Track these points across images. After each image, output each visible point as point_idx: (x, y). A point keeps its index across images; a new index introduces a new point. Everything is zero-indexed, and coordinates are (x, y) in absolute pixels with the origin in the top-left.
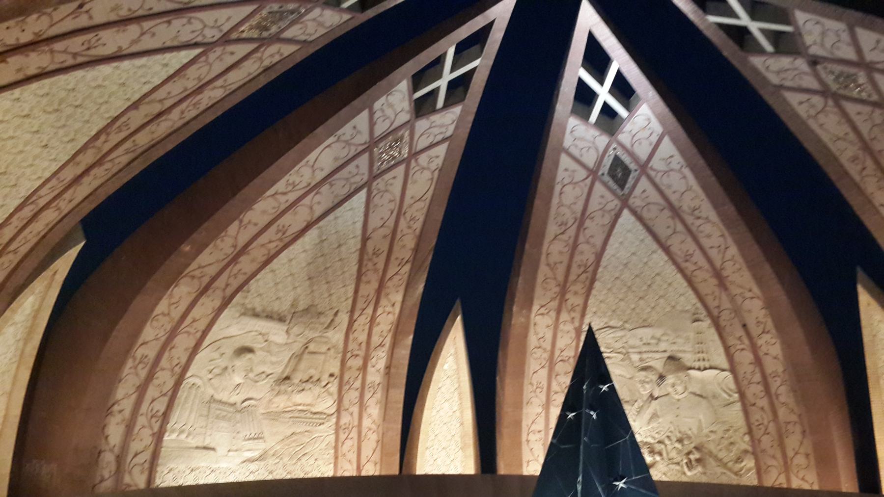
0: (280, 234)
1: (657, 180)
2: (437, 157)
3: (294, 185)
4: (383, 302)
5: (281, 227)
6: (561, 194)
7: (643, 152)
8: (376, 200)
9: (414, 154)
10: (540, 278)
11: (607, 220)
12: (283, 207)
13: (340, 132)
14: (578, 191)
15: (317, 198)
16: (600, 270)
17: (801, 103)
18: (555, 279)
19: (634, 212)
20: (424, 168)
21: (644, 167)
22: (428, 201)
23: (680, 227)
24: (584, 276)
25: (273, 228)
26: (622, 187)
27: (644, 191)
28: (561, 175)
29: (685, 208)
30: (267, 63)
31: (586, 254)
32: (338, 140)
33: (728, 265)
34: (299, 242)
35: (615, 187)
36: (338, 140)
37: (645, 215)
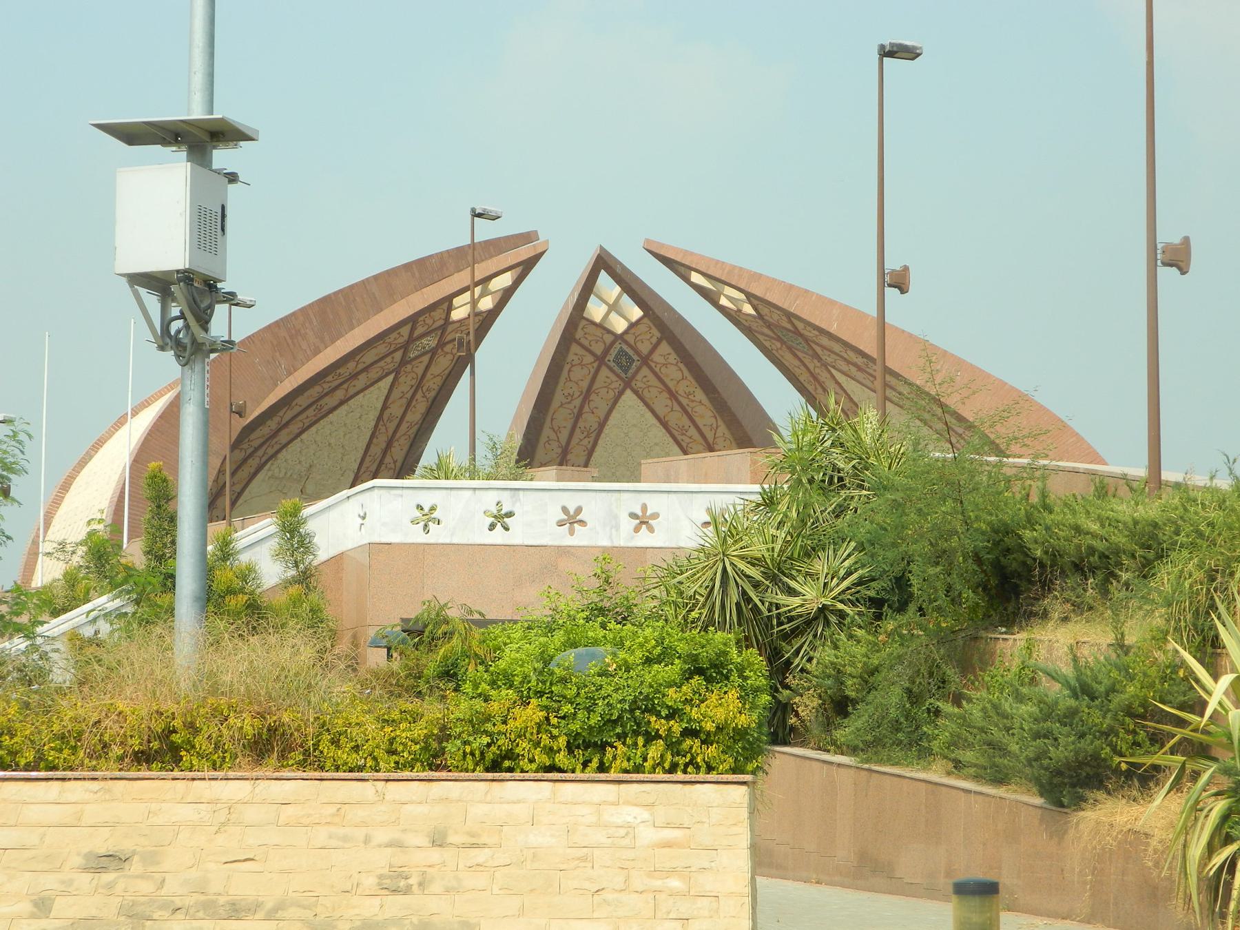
1: (657, 370)
4: (388, 460)
7: (644, 348)
8: (402, 379)
9: (441, 344)
10: (543, 439)
11: (611, 394)
14: (585, 371)
15: (355, 382)
19: (636, 392)
21: (646, 360)
24: (586, 440)
26: (626, 372)
28: (571, 357)
31: (589, 421)
35: (619, 371)
37: (646, 394)
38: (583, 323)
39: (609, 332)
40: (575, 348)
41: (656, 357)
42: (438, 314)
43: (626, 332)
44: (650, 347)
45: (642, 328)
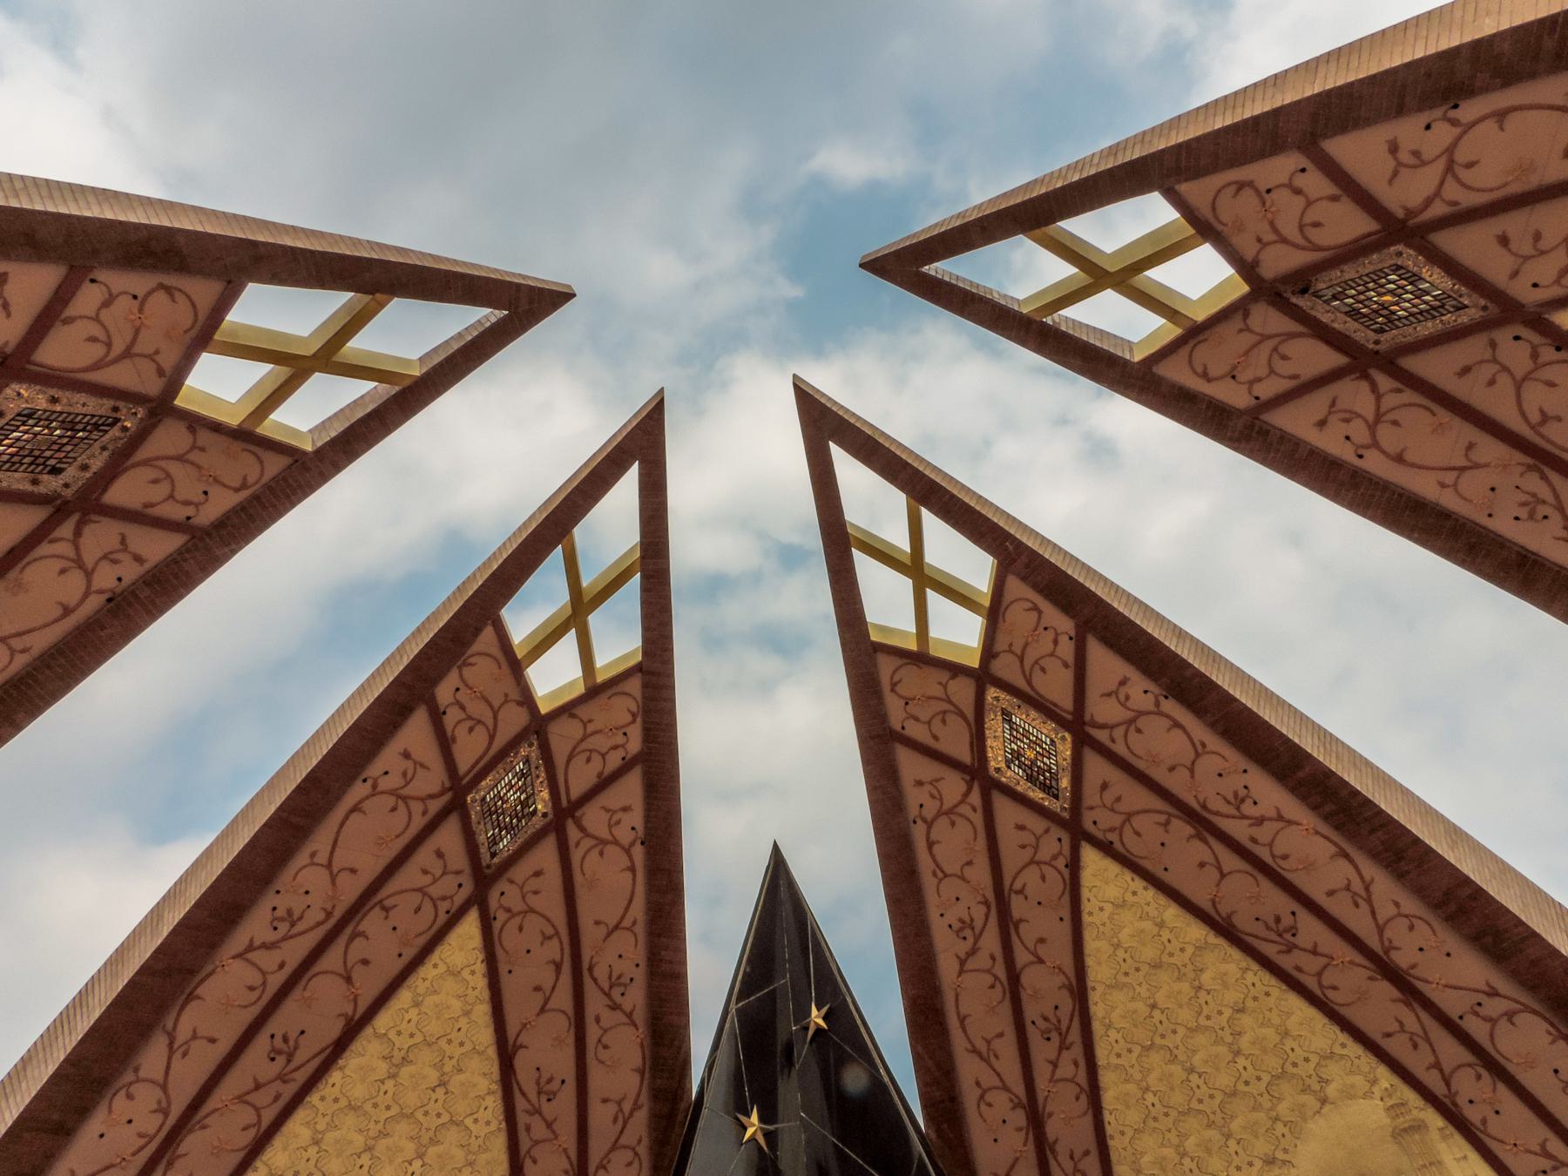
0: (281, 1060)
1: (1119, 748)
2: (625, 809)
3: (292, 918)
5: (278, 1042)
6: (930, 845)
7: (1057, 686)
8: (510, 939)
10: (969, 1095)
11: (1056, 882)
12: (276, 981)
13: (374, 770)
14: (963, 828)
15: (359, 949)
16: (1097, 1027)
17: (1322, 424)
18: (1006, 1088)
19: (1107, 849)
20: (602, 842)
21: (1077, 725)
22: (640, 929)
23: (1230, 861)
24: (1067, 1056)
25: (261, 1044)
27: (1104, 786)
28: (914, 798)
29: (1216, 804)
30: (106, 578)
31: (1044, 989)
32: (375, 790)
33: (1397, 932)
34: (335, 1076)
36: (375, 790)
37: (1134, 846)
38: (886, 666)
39: (955, 670)
40: (911, 766)
41: (1101, 709)
42: (481, 670)
43: (989, 651)
44: (1068, 676)
45: (1018, 618)
